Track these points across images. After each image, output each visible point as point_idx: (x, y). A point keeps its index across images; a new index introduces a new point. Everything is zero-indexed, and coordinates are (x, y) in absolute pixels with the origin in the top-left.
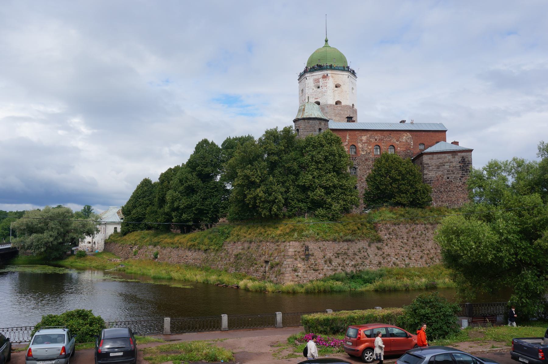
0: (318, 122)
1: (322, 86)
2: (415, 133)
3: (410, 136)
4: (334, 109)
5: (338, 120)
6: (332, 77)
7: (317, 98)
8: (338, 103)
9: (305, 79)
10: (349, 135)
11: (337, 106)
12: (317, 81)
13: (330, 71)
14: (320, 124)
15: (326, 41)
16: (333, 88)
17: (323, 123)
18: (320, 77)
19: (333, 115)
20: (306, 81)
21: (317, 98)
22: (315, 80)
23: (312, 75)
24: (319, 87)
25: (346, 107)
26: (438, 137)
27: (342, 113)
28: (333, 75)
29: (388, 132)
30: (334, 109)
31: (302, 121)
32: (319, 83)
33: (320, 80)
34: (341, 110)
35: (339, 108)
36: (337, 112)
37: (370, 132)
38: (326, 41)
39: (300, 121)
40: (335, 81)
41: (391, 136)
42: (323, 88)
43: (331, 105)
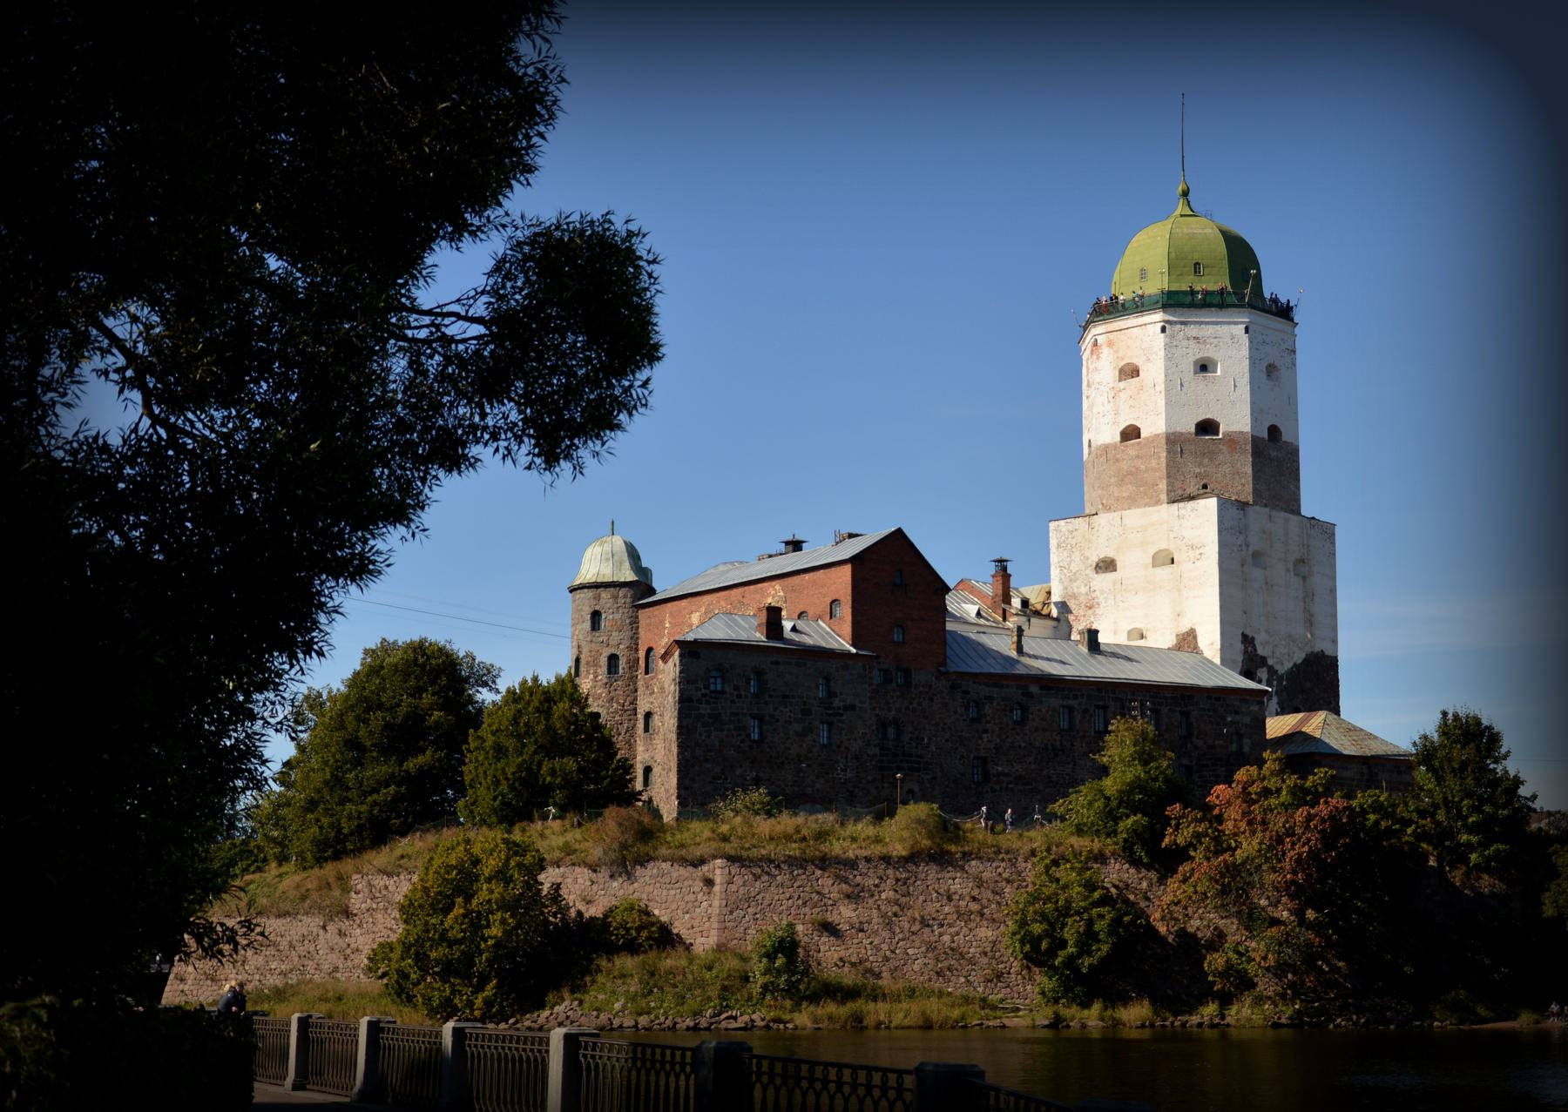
0: (589, 593)
2: (790, 581)
3: (782, 594)
4: (1117, 460)
5: (1129, 498)
6: (1110, 344)
8: (1131, 433)
10: (671, 615)
11: (1126, 446)
13: (1103, 326)
14: (598, 598)
16: (1111, 385)
17: (606, 595)
19: (1113, 480)
25: (1153, 441)
26: (835, 583)
27: (1143, 467)
28: (1111, 336)
29: (741, 590)
30: (1117, 460)
34: (1138, 457)
35: (1132, 453)
36: (1124, 466)
37: (707, 598)
40: (1120, 355)
41: (745, 601)
43: (1106, 449)
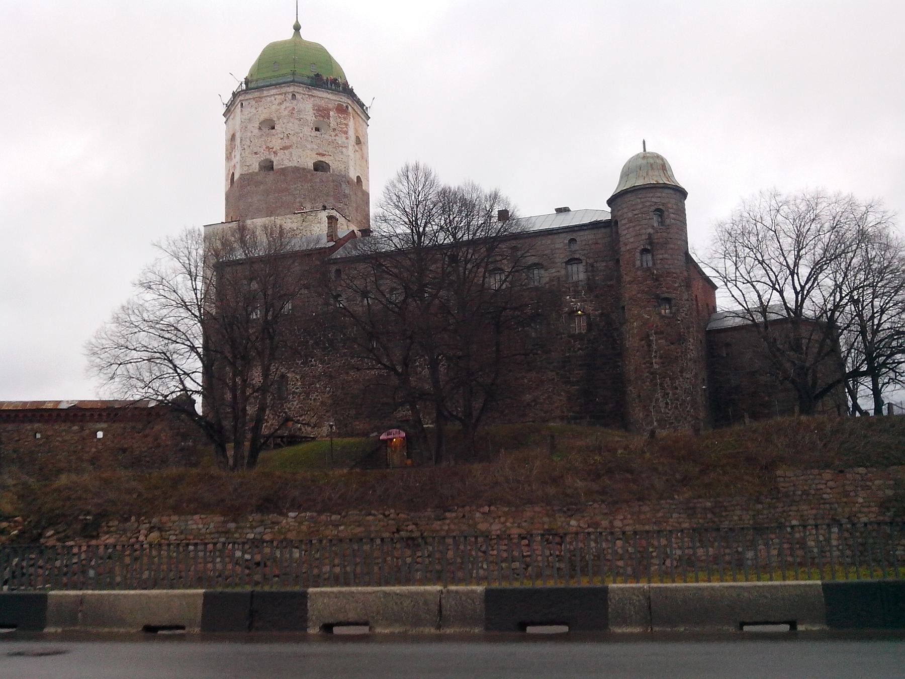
1: (334, 130)
7: (324, 155)
9: (290, 96)
12: (322, 112)
15: (297, 28)
18: (330, 106)
20: (295, 102)
21: (324, 155)
22: (318, 110)
23: (310, 94)
24: (317, 129)
31: (671, 191)
32: (328, 118)
33: (331, 113)
38: (297, 28)
39: (666, 191)
42: (336, 135)
